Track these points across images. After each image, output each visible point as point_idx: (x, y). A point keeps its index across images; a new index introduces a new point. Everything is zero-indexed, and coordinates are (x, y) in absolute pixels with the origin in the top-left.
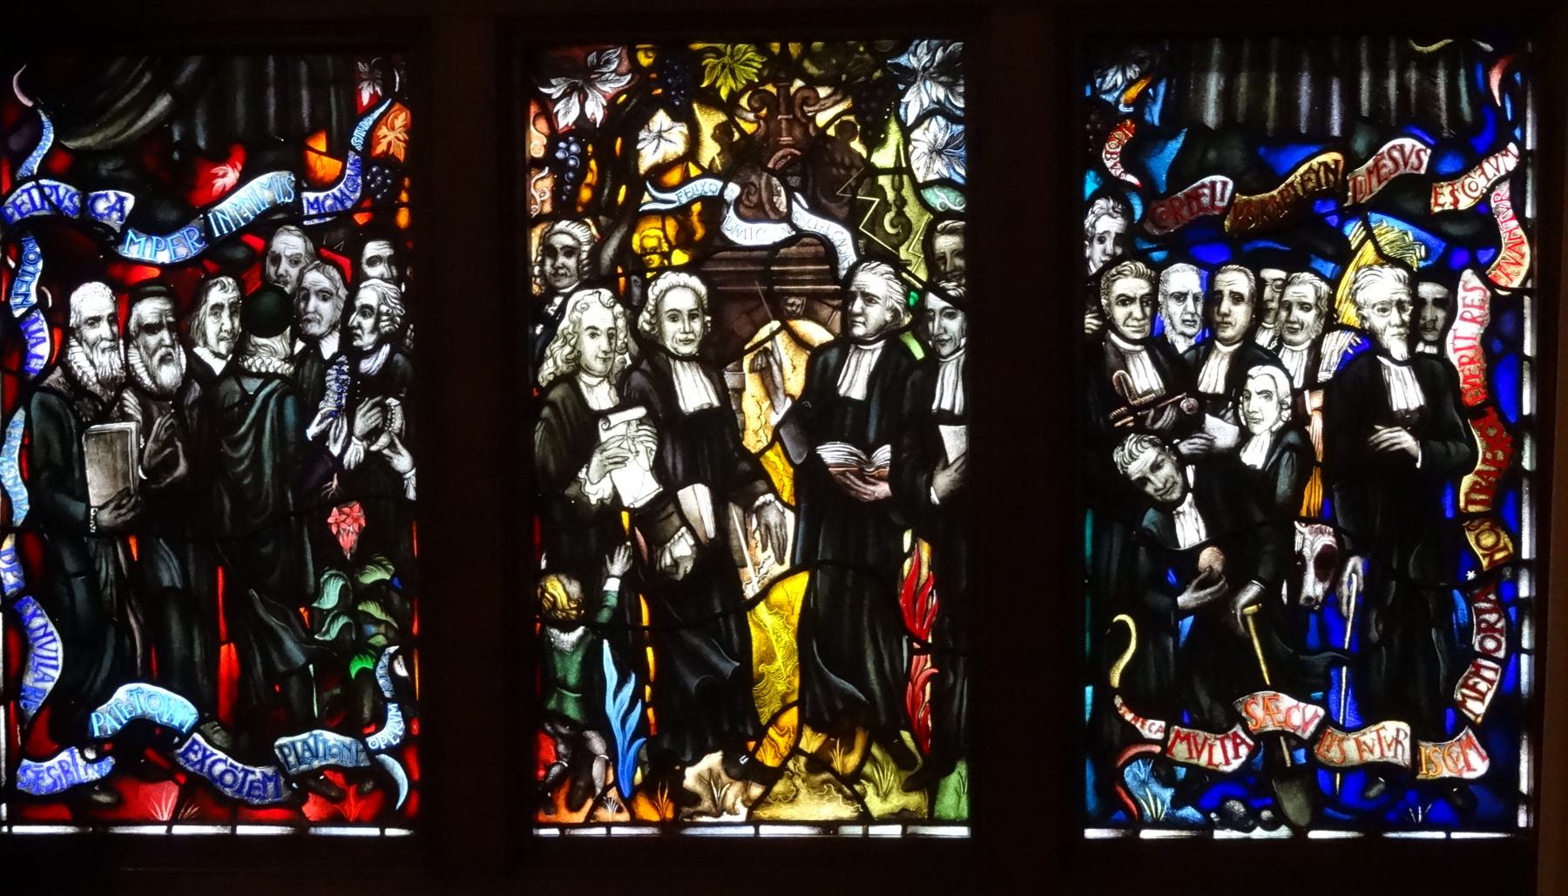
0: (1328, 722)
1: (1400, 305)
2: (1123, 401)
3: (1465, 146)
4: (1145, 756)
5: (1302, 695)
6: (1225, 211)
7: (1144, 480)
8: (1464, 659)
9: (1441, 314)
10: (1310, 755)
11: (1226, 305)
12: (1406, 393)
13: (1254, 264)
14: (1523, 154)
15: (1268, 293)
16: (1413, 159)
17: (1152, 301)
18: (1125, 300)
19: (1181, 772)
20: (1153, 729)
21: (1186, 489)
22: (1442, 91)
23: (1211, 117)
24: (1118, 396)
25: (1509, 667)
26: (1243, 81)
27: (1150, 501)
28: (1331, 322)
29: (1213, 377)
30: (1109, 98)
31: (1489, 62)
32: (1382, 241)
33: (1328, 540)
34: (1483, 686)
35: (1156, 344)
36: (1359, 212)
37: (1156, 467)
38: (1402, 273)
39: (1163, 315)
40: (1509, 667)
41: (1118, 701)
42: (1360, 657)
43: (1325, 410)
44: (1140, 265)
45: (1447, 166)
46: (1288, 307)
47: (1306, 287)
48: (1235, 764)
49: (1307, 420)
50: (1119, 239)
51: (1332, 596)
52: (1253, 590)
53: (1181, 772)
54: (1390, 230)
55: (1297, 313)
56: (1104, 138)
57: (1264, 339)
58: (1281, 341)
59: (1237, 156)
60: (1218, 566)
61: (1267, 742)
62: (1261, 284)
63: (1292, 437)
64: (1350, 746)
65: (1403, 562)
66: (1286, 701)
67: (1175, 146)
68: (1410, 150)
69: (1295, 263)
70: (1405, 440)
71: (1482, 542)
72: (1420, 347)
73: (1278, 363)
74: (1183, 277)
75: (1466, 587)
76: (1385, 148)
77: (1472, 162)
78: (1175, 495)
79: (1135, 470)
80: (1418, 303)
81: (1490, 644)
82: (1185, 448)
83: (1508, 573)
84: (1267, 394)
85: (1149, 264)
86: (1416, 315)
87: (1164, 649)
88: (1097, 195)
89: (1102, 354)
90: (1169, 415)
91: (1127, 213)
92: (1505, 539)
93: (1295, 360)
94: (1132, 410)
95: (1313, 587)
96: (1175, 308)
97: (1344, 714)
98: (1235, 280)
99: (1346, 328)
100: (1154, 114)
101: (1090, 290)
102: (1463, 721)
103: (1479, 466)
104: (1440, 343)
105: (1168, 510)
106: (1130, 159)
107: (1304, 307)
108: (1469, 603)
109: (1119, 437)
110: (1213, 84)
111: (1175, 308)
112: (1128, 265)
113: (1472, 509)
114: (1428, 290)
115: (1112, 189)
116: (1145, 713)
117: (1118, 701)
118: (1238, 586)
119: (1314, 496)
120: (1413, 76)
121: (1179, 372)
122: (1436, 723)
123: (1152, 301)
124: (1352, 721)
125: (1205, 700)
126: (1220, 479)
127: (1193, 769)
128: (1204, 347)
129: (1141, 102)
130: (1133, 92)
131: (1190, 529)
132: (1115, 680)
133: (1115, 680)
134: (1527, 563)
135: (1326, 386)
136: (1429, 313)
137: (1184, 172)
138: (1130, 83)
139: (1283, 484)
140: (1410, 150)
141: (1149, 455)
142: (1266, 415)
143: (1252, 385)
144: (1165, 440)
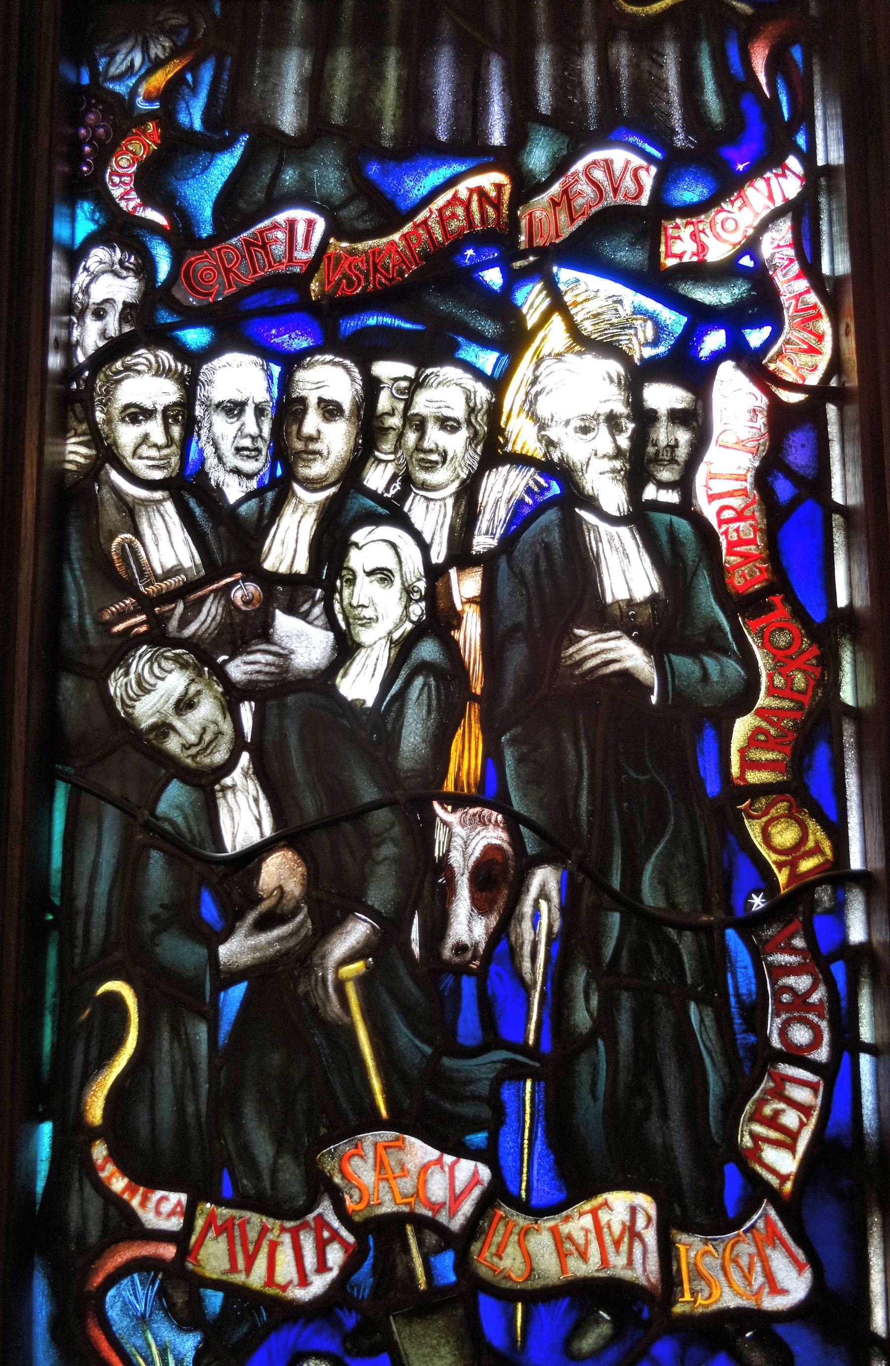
0: (496, 1195)
1: (613, 421)
2: (128, 588)
3: (717, 161)
4: (144, 1266)
5: (450, 1143)
6: (313, 266)
7: (163, 729)
8: (754, 1066)
9: (683, 436)
10: (463, 1264)
11: (312, 422)
12: (627, 572)
13: (362, 351)
14: (814, 175)
15: (384, 402)
16: (628, 183)
17: (184, 416)
18: (137, 414)
19: (214, 1300)
20: (161, 1210)
21: (239, 745)
22: (672, 77)
23: (289, 118)
24: (120, 578)
25: (836, 1077)
26: (342, 64)
27: (175, 769)
28: (493, 451)
29: (289, 545)
30: (121, 89)
31: (748, 33)
32: (579, 315)
33: (495, 835)
34: (791, 1119)
35: (188, 487)
36: (542, 263)
37: (185, 705)
38: (615, 367)
39: (201, 443)
40: (836, 1077)
41: (99, 1151)
42: (556, 1064)
43: (486, 601)
44: (166, 357)
45: (689, 193)
46: (421, 426)
47: (449, 391)
48: (319, 1284)
49: (455, 619)
50: (128, 311)
51: (501, 935)
52: (358, 931)
53: (214, 1300)
54: (594, 294)
55: (435, 436)
56: (106, 152)
57: (377, 478)
58: (407, 482)
59: (330, 177)
60: (294, 887)
61: (380, 1236)
62: (372, 386)
63: (428, 650)
64: (541, 1243)
65: (632, 875)
66: (419, 1151)
67: (226, 164)
68: (622, 168)
69: (431, 349)
70: (630, 655)
71: (777, 836)
72: (650, 492)
73: (403, 522)
74: (239, 376)
75: (749, 925)
76: (579, 166)
77: (726, 186)
78: (220, 756)
79: (146, 711)
80: (645, 418)
81: (801, 1035)
82: (237, 670)
83: (824, 895)
84: (383, 575)
85: (181, 352)
86: (641, 438)
87: (189, 1050)
88: (92, 241)
89: (93, 505)
90: (210, 613)
91: (145, 268)
92: (816, 834)
93: (432, 516)
94: (145, 604)
95: (467, 926)
96: (223, 428)
97: (532, 1172)
98: (329, 380)
99: (521, 460)
100: (193, 116)
101: (77, 397)
102: (758, 1190)
103: (763, 700)
104: (685, 485)
105: (207, 783)
106: (154, 182)
107: (447, 424)
108: (757, 955)
109: (121, 651)
110: (293, 69)
111: (223, 428)
112: (143, 356)
113: (754, 777)
114: (663, 397)
115: (119, 231)
116: (148, 1177)
117: (99, 1151)
118: (328, 924)
119: (467, 756)
120: (623, 54)
121: (230, 537)
122: (705, 1198)
123: (184, 416)
124: (546, 1191)
125: (264, 1150)
126: (298, 728)
127: (235, 1293)
128: (276, 491)
129: (171, 95)
130: (159, 79)
131: (244, 817)
132: (96, 1110)
133: (96, 1110)
134: (863, 879)
135: (488, 562)
136: (663, 434)
137: (239, 207)
138: (156, 65)
139: (413, 734)
140: (622, 168)
141: (175, 682)
142: (382, 610)
143: (357, 560)
144: (203, 657)
